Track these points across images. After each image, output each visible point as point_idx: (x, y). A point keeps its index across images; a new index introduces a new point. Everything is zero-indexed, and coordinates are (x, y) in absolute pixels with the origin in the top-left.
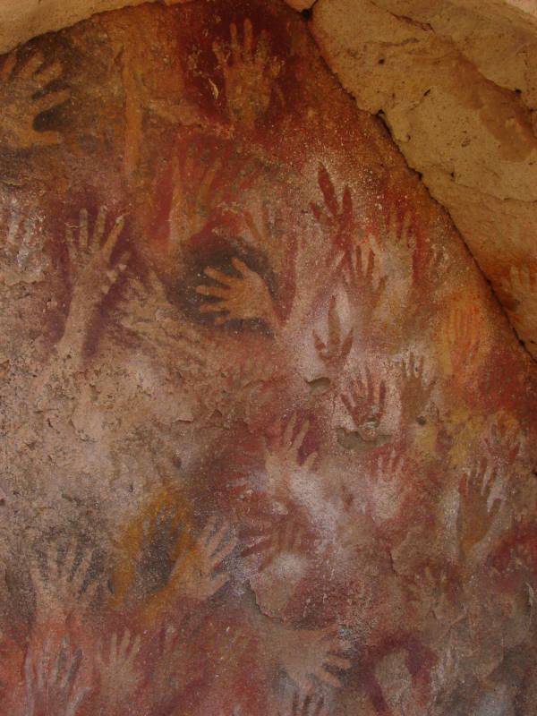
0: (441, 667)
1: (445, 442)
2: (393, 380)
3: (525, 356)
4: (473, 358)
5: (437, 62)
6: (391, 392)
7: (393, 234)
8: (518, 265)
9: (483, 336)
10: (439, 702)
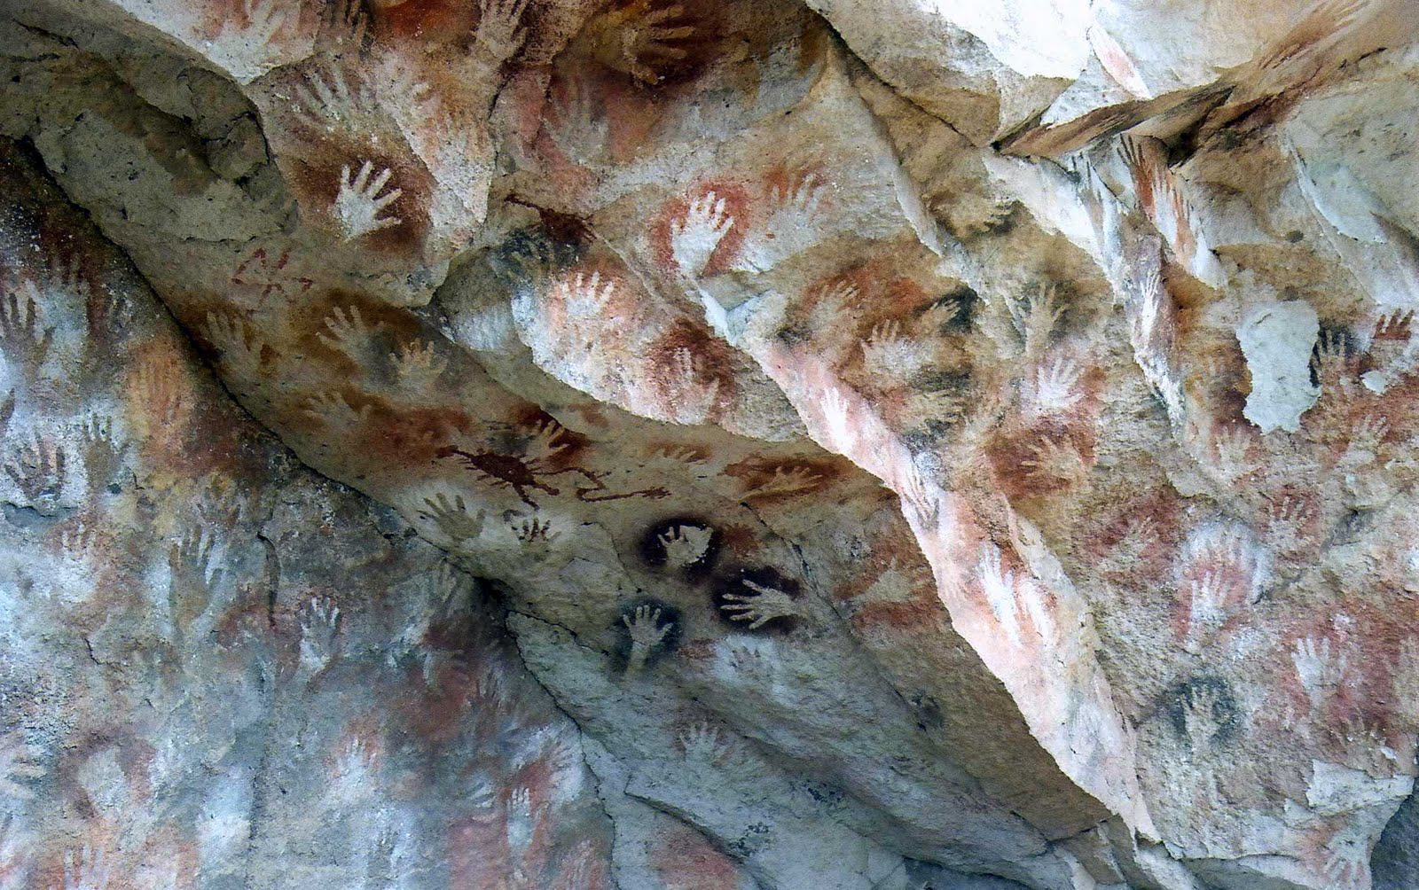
0: (162, 759)
1: (148, 510)
2: (74, 444)
3: (237, 410)
4: (174, 417)
5: (86, 83)
6: (72, 459)
7: (59, 281)
8: (214, 311)
9: (184, 392)
10: (161, 798)
